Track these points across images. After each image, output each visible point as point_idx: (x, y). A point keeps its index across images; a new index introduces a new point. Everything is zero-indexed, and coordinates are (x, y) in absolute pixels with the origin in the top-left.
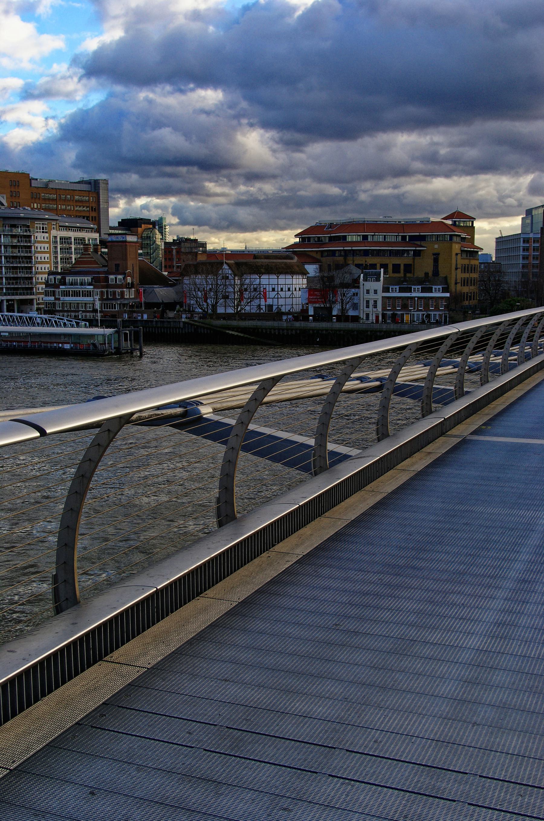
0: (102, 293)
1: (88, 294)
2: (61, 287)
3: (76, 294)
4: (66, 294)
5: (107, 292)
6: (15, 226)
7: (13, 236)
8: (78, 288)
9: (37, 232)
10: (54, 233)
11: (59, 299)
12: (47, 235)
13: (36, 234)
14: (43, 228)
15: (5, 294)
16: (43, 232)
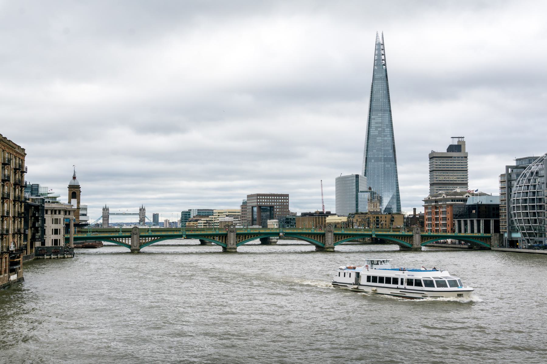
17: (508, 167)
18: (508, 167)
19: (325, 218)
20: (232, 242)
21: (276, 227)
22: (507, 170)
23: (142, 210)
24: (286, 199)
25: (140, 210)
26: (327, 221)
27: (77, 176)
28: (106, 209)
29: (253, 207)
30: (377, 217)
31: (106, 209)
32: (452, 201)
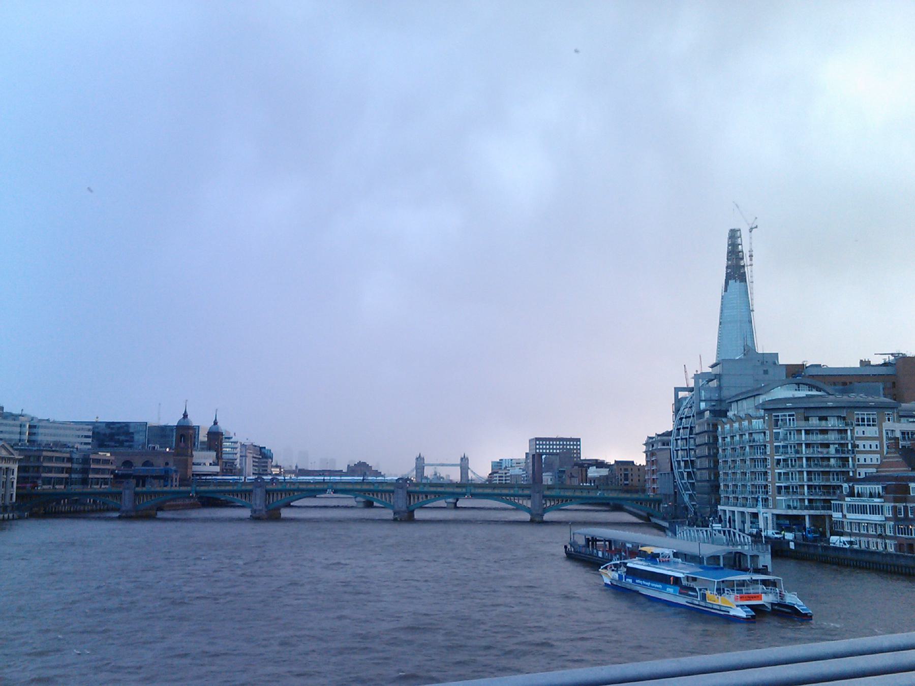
0: (895, 510)
1: (875, 510)
2: (847, 499)
3: (863, 510)
4: (853, 509)
5: (906, 508)
6: (824, 418)
7: (824, 432)
8: (866, 502)
9: (858, 425)
10: (887, 425)
11: (844, 516)
12: (876, 428)
13: (857, 429)
14: (869, 420)
15: (806, 508)
16: (869, 425)
17: (677, 390)
18: (677, 390)
19: (586, 471)
20: (258, 502)
21: (550, 483)
22: (676, 395)
23: (464, 460)
24: (577, 445)
25: (462, 459)
26: (590, 475)
27: (188, 413)
28: (420, 459)
29: (533, 456)
30: (626, 470)
31: (420, 459)
32: (664, 445)
